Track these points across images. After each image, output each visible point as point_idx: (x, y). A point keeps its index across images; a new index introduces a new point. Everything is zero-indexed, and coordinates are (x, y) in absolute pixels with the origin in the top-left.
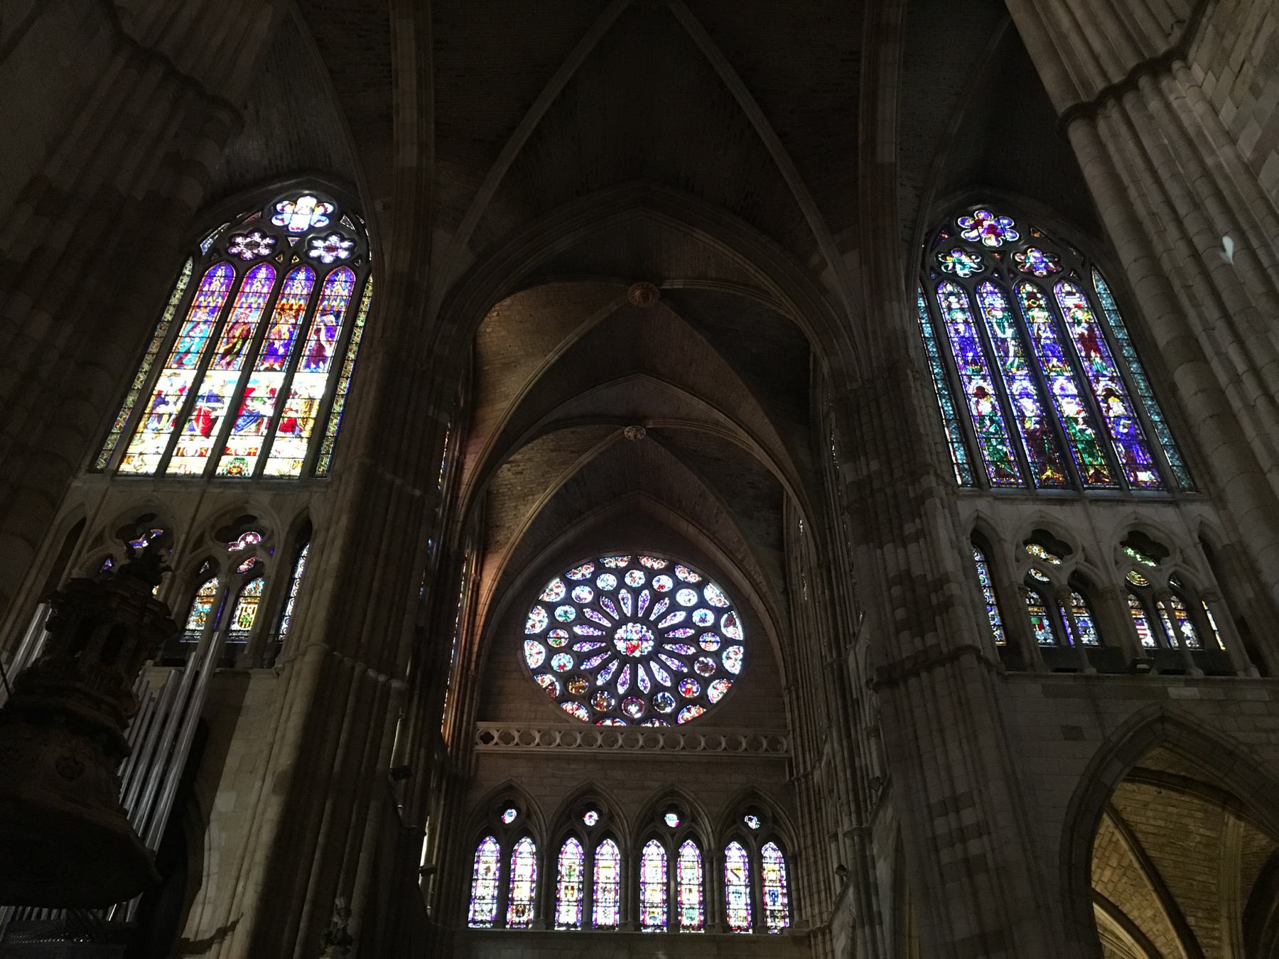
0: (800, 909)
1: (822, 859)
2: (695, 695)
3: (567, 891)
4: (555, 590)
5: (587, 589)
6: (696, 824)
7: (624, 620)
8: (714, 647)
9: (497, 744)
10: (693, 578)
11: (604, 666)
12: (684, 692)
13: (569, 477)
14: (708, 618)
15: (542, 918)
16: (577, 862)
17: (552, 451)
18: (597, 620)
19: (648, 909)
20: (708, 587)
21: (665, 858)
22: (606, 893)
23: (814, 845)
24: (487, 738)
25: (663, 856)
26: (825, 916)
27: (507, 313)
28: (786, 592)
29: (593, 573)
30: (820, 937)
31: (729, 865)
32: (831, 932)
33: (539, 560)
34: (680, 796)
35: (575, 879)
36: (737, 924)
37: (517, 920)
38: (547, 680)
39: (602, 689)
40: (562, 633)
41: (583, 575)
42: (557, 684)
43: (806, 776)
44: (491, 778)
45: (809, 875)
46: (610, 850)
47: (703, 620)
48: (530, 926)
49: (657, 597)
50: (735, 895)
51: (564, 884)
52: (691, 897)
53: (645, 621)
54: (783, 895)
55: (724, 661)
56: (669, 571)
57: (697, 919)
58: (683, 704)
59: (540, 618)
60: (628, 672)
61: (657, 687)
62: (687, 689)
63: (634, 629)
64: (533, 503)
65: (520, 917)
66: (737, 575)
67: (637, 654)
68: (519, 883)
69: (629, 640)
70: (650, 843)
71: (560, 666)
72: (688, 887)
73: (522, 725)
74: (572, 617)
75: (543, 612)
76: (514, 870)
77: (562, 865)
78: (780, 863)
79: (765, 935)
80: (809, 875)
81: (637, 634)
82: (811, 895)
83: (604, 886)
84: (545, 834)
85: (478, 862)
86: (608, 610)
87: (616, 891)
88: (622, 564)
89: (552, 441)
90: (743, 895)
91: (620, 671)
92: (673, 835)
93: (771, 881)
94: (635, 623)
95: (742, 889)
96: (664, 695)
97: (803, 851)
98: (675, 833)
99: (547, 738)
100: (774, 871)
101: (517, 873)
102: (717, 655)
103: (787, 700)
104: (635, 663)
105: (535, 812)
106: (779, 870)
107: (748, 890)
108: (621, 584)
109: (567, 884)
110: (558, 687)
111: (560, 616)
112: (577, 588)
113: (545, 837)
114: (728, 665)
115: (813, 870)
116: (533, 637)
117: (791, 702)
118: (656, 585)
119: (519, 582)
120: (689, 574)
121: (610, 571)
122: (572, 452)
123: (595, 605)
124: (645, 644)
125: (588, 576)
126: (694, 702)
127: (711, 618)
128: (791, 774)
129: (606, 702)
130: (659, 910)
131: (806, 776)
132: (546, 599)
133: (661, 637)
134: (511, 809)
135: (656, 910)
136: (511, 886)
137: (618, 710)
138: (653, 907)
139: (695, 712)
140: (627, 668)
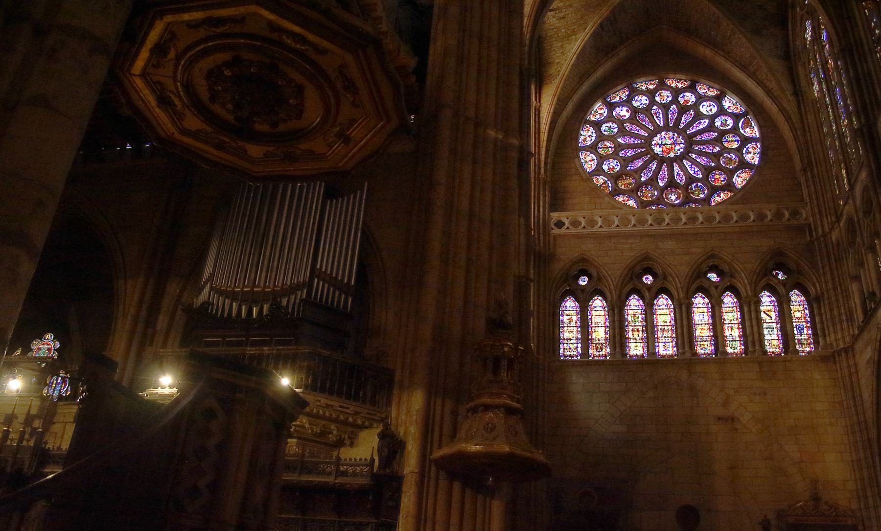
0: (824, 337)
1: (843, 297)
2: (723, 183)
3: (634, 333)
4: (599, 111)
5: (625, 109)
6: (735, 278)
7: (658, 130)
8: (735, 145)
9: (568, 228)
10: (713, 93)
11: (645, 166)
12: (714, 181)
13: (603, 17)
14: (728, 123)
15: (618, 350)
18: (636, 132)
19: (699, 343)
20: (726, 98)
21: (710, 306)
22: (665, 333)
23: (835, 289)
24: (560, 224)
25: (707, 304)
26: (847, 339)
29: (628, 96)
31: (762, 308)
32: (853, 350)
33: (585, 87)
34: (721, 259)
35: (639, 324)
36: (771, 350)
37: (598, 354)
38: (601, 180)
39: (646, 183)
40: (608, 144)
41: (620, 98)
42: (609, 182)
43: (824, 236)
44: (567, 253)
45: (831, 310)
46: (665, 302)
47: (724, 124)
48: (608, 358)
49: (683, 109)
50: (768, 329)
51: (631, 328)
52: (733, 333)
53: (675, 129)
55: (744, 156)
56: (692, 88)
57: (739, 348)
58: (714, 190)
59: (590, 134)
60: (666, 169)
61: (691, 180)
62: (715, 179)
63: (667, 136)
64: (576, 41)
65: (599, 352)
66: (750, 84)
67: (672, 155)
68: (597, 329)
69: (664, 145)
70: (697, 295)
71: (609, 169)
72: (730, 325)
73: (584, 213)
74: (616, 130)
75: (591, 129)
76: (591, 319)
77: (627, 315)
78: (803, 305)
79: (798, 356)
80: (831, 310)
81: (670, 140)
82: (834, 325)
83: (663, 327)
84: (614, 292)
86: (644, 123)
87: (672, 331)
88: (651, 87)
90: (775, 330)
91: (659, 168)
92: (716, 287)
93: (797, 318)
94: (668, 131)
95: (774, 325)
96: (697, 185)
97: (825, 293)
98: (718, 286)
99: (608, 222)
100: (799, 311)
102: (739, 150)
103: (802, 181)
104: (670, 162)
105: (605, 277)
106: (803, 310)
107: (778, 326)
108: (653, 102)
109: (634, 328)
110: (610, 185)
111: (605, 131)
112: (617, 109)
113: (614, 294)
114: (748, 157)
115: (835, 305)
116: (585, 149)
117: (807, 181)
118: (681, 101)
119: (570, 107)
120: (709, 89)
121: (642, 93)
123: (633, 120)
124: (677, 147)
125: (625, 99)
126: (722, 189)
127: (730, 122)
128: (811, 236)
129: (649, 194)
130: (708, 343)
131: (824, 236)
132: (593, 119)
133: (690, 142)
134: (584, 276)
135: (706, 343)
136: (590, 330)
137: (661, 199)
138: (703, 341)
139: (723, 196)
140: (665, 168)
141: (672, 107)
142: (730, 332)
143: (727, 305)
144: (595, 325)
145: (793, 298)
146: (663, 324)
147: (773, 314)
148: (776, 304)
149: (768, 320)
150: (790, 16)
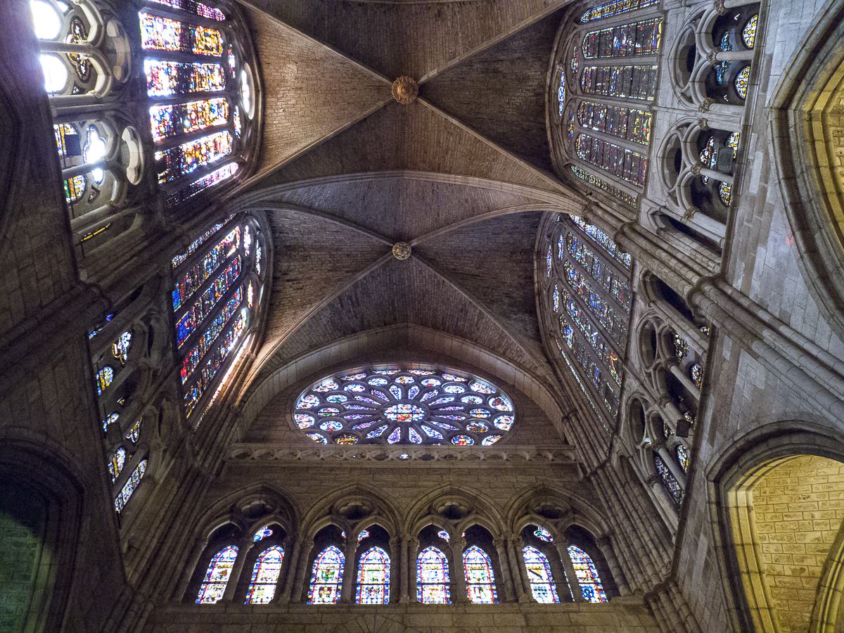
3: (322, 592)
16: (337, 566)
17: (330, 271)
21: (447, 561)
22: (372, 593)
25: (444, 560)
27: (292, 110)
28: (549, 362)
30: (662, 596)
32: (676, 585)
38: (315, 437)
46: (379, 556)
50: (538, 592)
54: (599, 591)
66: (501, 364)
67: (408, 420)
70: (428, 549)
76: (257, 574)
77: (317, 569)
82: (638, 563)
85: (213, 567)
89: (330, 262)
90: (549, 592)
94: (405, 403)
95: (547, 587)
97: (616, 528)
101: (260, 576)
107: (554, 587)
109: (323, 586)
122: (347, 272)
131: (602, 466)
141: (413, 388)
142: (478, 595)
143: (473, 562)
144: (260, 582)
145: (571, 555)
146: (371, 582)
147: (543, 573)
148: (547, 561)
149: (536, 579)
150: (537, 302)
